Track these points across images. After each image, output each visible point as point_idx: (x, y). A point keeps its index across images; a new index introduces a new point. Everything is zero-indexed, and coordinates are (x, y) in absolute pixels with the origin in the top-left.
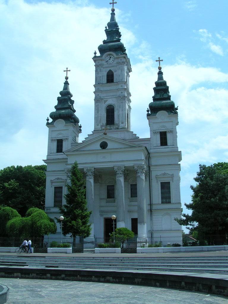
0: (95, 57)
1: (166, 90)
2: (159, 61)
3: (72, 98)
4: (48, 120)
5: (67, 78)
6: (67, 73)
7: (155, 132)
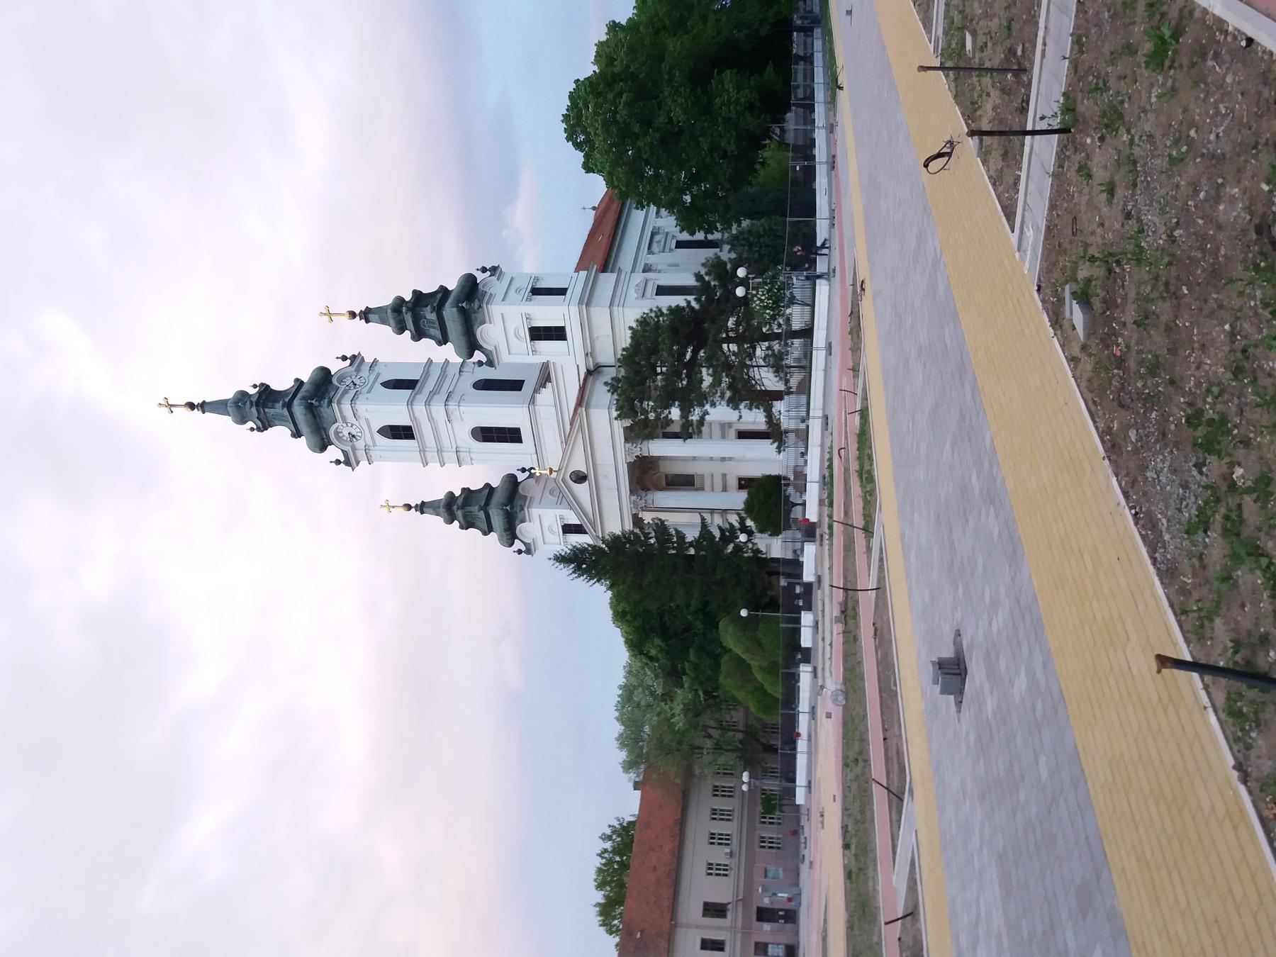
0: (347, 463)
3: (457, 493)
4: (520, 552)
7: (533, 351)
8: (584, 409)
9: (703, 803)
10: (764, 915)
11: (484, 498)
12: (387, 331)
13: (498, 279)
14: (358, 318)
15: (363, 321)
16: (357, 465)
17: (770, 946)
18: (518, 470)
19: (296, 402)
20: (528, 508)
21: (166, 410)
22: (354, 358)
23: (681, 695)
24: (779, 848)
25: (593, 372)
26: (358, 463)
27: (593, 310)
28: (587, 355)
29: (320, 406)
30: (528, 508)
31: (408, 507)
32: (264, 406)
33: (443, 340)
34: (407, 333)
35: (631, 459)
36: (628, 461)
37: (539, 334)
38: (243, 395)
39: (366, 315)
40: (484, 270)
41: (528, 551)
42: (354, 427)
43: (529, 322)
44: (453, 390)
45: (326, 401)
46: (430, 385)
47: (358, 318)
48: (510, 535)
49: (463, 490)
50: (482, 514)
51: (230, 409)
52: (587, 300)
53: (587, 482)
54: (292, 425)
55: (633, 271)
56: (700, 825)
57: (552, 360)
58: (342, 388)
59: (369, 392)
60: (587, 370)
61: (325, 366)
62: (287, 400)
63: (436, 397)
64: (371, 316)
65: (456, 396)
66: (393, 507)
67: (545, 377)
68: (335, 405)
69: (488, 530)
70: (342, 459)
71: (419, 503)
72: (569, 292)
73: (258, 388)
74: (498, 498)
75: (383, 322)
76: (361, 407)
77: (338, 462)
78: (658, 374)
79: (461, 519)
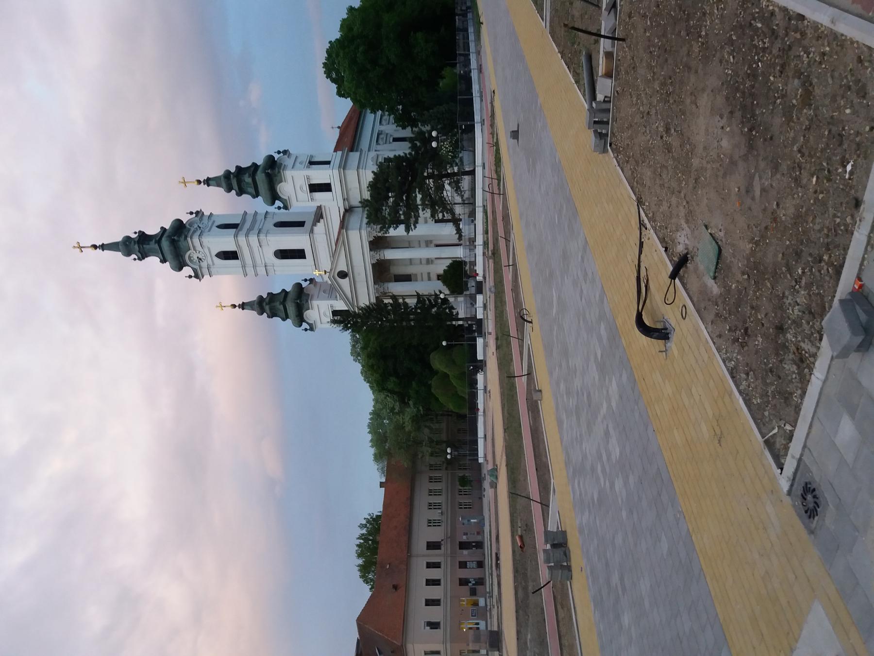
0: (197, 276)
2: (185, 183)
3: (265, 296)
4: (306, 330)
8: (345, 230)
9: (423, 487)
10: (463, 546)
11: (283, 297)
12: (220, 191)
13: (288, 157)
14: (202, 184)
15: (206, 186)
16: (203, 277)
17: (468, 563)
18: (302, 280)
19: (163, 239)
20: (311, 300)
21: (78, 250)
22: (197, 213)
23: (411, 411)
24: (470, 494)
25: (349, 211)
26: (203, 277)
27: (347, 172)
28: (344, 200)
29: (178, 241)
30: (311, 300)
31: (234, 306)
32: (143, 244)
33: (256, 195)
34: (233, 192)
35: (374, 262)
36: (372, 263)
37: (315, 188)
38: (127, 239)
39: (208, 182)
40: (279, 152)
41: (312, 329)
42: (201, 253)
44: (262, 227)
45: (183, 237)
46: (247, 225)
47: (202, 184)
48: (300, 320)
49: (269, 294)
50: (281, 307)
51: (120, 247)
52: (343, 166)
53: (348, 278)
54: (161, 255)
55: (369, 150)
56: (422, 499)
57: (323, 204)
58: (192, 229)
59: (209, 231)
60: (345, 209)
61: (180, 219)
62: (157, 239)
63: (251, 232)
64: (210, 182)
65: (264, 231)
66: (225, 307)
67: (319, 215)
68: (189, 239)
69: (285, 317)
70: (193, 274)
71: (241, 303)
72: (332, 163)
73: (137, 234)
74: (290, 297)
75: (219, 185)
76: (206, 240)
77: (190, 277)
78: (390, 197)
79: (268, 311)
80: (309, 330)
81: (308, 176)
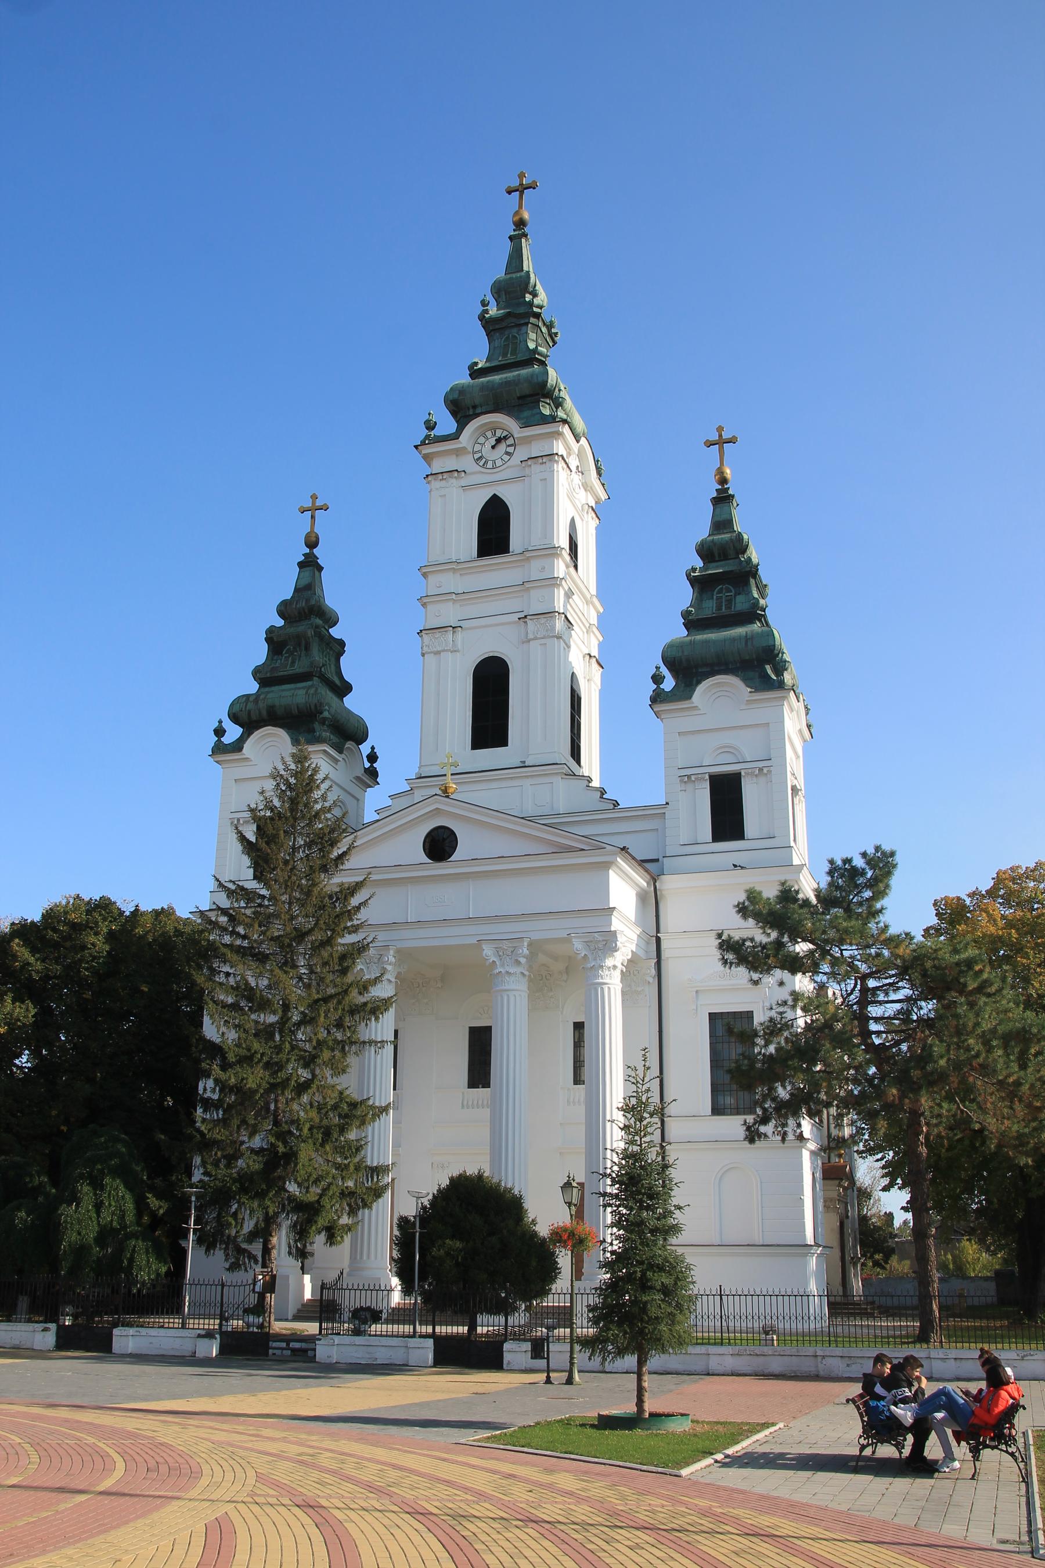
1: (746, 575)
3: (335, 632)
4: (219, 732)
5: (312, 543)
6: (313, 517)
7: (689, 776)
43: (752, 774)
49: (341, 644)
80: (219, 740)
81: (769, 772)
